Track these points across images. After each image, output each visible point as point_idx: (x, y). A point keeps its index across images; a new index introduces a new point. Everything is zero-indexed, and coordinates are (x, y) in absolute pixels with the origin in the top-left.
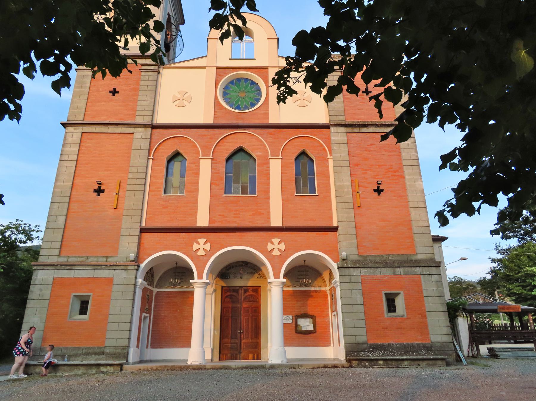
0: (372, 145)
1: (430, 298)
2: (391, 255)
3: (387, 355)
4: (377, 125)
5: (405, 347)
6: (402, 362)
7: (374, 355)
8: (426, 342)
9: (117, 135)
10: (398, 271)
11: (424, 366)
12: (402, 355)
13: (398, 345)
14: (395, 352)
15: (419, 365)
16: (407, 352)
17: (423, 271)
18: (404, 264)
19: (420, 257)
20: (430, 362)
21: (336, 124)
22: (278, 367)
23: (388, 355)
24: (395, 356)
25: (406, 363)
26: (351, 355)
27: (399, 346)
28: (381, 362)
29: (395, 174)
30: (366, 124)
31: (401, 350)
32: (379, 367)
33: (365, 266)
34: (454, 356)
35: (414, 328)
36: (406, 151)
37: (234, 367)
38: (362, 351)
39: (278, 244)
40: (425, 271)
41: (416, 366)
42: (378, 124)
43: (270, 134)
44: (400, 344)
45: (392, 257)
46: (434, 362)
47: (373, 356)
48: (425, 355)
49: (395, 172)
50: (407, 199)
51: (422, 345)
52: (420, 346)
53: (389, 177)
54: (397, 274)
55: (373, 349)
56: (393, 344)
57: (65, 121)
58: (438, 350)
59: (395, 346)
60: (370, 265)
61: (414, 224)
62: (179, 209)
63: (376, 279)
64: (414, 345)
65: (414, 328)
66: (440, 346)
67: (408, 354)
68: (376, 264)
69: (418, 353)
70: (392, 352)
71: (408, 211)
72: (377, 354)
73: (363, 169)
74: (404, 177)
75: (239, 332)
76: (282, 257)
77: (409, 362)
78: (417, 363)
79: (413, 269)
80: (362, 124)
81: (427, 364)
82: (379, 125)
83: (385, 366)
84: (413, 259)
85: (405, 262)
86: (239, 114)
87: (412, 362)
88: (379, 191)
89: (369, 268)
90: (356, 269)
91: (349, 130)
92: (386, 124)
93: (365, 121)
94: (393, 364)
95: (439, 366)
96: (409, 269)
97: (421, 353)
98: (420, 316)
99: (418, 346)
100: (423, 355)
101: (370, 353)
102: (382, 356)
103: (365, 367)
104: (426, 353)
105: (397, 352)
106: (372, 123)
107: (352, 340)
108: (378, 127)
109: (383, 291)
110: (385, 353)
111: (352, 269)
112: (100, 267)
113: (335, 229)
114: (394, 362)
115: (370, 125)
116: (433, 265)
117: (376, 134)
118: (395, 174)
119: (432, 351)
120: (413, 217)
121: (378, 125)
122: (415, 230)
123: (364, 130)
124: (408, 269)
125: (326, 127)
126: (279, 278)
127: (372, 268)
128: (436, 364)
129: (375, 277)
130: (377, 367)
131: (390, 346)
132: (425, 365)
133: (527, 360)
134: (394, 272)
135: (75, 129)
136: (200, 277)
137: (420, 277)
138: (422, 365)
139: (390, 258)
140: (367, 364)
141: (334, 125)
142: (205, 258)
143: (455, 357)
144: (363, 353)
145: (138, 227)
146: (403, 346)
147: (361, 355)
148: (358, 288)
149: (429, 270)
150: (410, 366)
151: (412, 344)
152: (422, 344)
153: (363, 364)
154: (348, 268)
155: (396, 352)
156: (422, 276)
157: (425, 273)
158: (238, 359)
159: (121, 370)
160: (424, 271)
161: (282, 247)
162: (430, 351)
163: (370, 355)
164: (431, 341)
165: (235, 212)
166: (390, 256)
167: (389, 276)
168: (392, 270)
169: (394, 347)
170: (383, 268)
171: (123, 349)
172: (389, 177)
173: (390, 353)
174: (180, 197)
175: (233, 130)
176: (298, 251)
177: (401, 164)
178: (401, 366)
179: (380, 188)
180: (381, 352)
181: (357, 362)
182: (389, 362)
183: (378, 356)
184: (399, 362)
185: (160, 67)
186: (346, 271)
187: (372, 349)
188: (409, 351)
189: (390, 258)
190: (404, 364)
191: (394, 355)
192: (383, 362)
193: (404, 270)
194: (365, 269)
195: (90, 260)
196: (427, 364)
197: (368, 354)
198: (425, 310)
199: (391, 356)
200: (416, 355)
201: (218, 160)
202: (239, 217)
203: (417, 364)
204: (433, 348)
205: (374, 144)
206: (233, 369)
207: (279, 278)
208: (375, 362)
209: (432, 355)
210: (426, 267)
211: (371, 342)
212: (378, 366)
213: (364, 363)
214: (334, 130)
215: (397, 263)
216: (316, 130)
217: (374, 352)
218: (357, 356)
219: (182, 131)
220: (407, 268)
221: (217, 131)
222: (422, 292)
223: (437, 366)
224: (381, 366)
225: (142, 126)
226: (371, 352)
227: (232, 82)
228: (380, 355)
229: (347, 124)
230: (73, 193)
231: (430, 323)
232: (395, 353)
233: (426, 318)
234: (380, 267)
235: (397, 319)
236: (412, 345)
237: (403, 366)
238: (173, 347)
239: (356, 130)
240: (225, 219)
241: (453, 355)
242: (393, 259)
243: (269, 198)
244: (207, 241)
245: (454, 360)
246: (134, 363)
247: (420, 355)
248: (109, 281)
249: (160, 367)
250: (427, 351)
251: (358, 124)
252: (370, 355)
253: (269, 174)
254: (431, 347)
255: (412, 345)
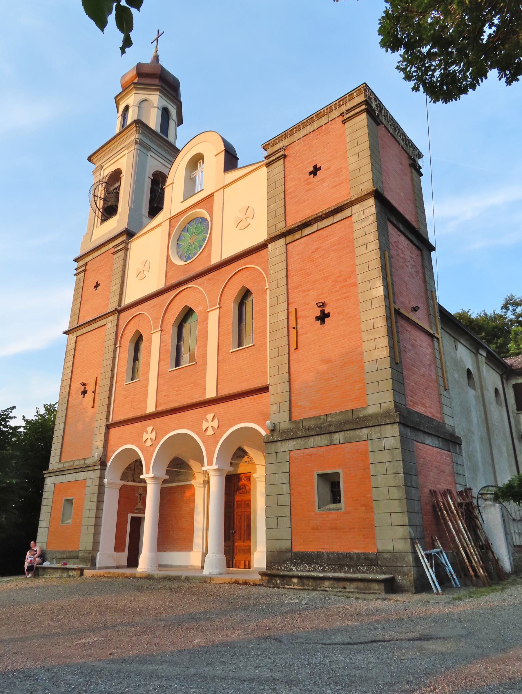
0: (316, 250)
1: (379, 478)
2: (330, 414)
3: (315, 570)
4: (321, 216)
5: (339, 558)
6: (321, 581)
7: (299, 570)
8: (371, 551)
9: (97, 330)
10: (338, 438)
11: (352, 590)
12: (335, 571)
13: (330, 555)
14: (325, 565)
15: (345, 588)
16: (341, 567)
17: (371, 434)
18: (344, 425)
19: (371, 410)
20: (361, 585)
21: (272, 238)
22: (192, 580)
23: (316, 570)
24: (325, 572)
25: (327, 583)
26: (271, 567)
27: (331, 557)
28: (295, 580)
29: (345, 283)
30: (305, 223)
31: (334, 563)
32: (292, 587)
33: (294, 437)
34: (411, 576)
35: (354, 528)
36: (361, 241)
37: (156, 576)
38: (284, 563)
39: (212, 421)
40: (375, 432)
41: (340, 590)
42: (321, 215)
43: (209, 280)
44: (332, 553)
45: (332, 418)
46: (366, 584)
47: (297, 571)
48: (367, 573)
49: (345, 280)
50: (359, 319)
51: (363, 556)
52: (360, 558)
53: (337, 291)
54: (335, 443)
55: (298, 561)
56: (323, 553)
57: (66, 328)
58: (387, 564)
59: (325, 556)
60: (300, 434)
61: (366, 357)
62: (135, 396)
63: (307, 455)
64: (352, 555)
65: (354, 528)
66: (390, 559)
67: (343, 570)
68: (307, 432)
69: (357, 569)
70: (321, 565)
71: (361, 338)
72: (302, 568)
73: (304, 291)
74: (355, 285)
75: (231, 532)
76: (216, 437)
77: (331, 582)
78: (341, 584)
79: (358, 432)
80: (301, 225)
81: (357, 588)
82: (325, 216)
83: (299, 586)
84: (361, 415)
85: (349, 422)
86: (186, 266)
87: (335, 583)
88: (323, 317)
89: (299, 439)
90: (284, 443)
91: (289, 238)
92: (331, 211)
93: (309, 218)
94: (310, 584)
95: (374, 591)
96: (352, 433)
97: (361, 569)
98: (364, 508)
99: (357, 557)
100: (364, 573)
101: (294, 566)
102: (308, 571)
103: (276, 586)
104: (368, 570)
105: (328, 565)
106: (313, 218)
107: (275, 547)
108: (324, 218)
109: (316, 471)
110: (313, 566)
111: (279, 444)
112: (78, 470)
113: (265, 389)
114: (311, 580)
115: (312, 221)
116: (386, 421)
117: (324, 230)
118: (345, 283)
119: (377, 566)
120: (366, 346)
121: (323, 216)
122: (368, 367)
123: (308, 231)
124: (350, 434)
125: (263, 246)
126: (212, 464)
127: (303, 439)
128: (370, 589)
129: (307, 451)
130: (291, 587)
131: (319, 555)
132: (353, 589)
133: (361, 591)
134: (331, 440)
135: (73, 335)
136: (148, 472)
137: (367, 445)
138: (349, 589)
139: (329, 419)
140: (278, 582)
141: (269, 241)
142: (152, 448)
143: (412, 578)
144: (285, 566)
145: (104, 423)
146: (337, 557)
147: (283, 568)
148: (285, 471)
149: (381, 431)
150: (332, 588)
151: (349, 553)
152: (363, 554)
153: (273, 581)
154: (274, 443)
155: (326, 566)
156: (369, 442)
157: (374, 437)
158: (231, 567)
159: (82, 574)
160: (373, 433)
161: (215, 424)
162: (375, 566)
163: (294, 568)
164: (377, 550)
165: (176, 389)
166: (330, 416)
167: (324, 449)
168: (329, 438)
169: (325, 558)
170: (317, 437)
171: (89, 553)
172: (337, 291)
173: (319, 567)
174: (137, 382)
175: (178, 289)
176: (231, 426)
177: (354, 264)
178: (320, 588)
179: (326, 312)
180: (308, 564)
181: (267, 578)
182: (306, 582)
183: (303, 571)
184: (318, 582)
185: (129, 242)
186: (273, 448)
187: (297, 559)
188: (344, 565)
189: (329, 419)
190: (324, 586)
191: (323, 571)
192: (298, 581)
193: (345, 434)
194: (295, 440)
195: (75, 464)
196: (357, 588)
197: (292, 567)
198: (371, 497)
199: (320, 572)
200: (354, 572)
201: (167, 330)
202: (180, 394)
203: (342, 587)
204: (379, 562)
205: (320, 248)
206: (156, 579)
207: (212, 464)
208: (288, 579)
209: (377, 573)
210: (376, 427)
211: (298, 548)
212: (291, 585)
213: (275, 580)
214: (272, 246)
215: (335, 426)
216: (254, 256)
217: (298, 565)
218: (278, 569)
219: (140, 307)
220: (348, 432)
221: (165, 296)
222: (369, 468)
223: (371, 592)
224: (295, 587)
225: (111, 314)
226: (295, 564)
227: (184, 230)
228: (306, 569)
229: (284, 233)
230: (70, 399)
231: (377, 519)
232: (325, 567)
233: (372, 512)
234: (313, 436)
235: (331, 514)
236: (350, 555)
237: (322, 589)
238: (174, 551)
239: (297, 235)
240: (170, 398)
241: (410, 575)
242: (333, 419)
243: (206, 364)
244: (153, 428)
245: (410, 583)
246: (100, 568)
247: (360, 572)
248: (84, 481)
249: (106, 573)
250: (371, 566)
251: (296, 227)
252: (294, 568)
253: (207, 332)
254: (377, 559)
255: (350, 555)
